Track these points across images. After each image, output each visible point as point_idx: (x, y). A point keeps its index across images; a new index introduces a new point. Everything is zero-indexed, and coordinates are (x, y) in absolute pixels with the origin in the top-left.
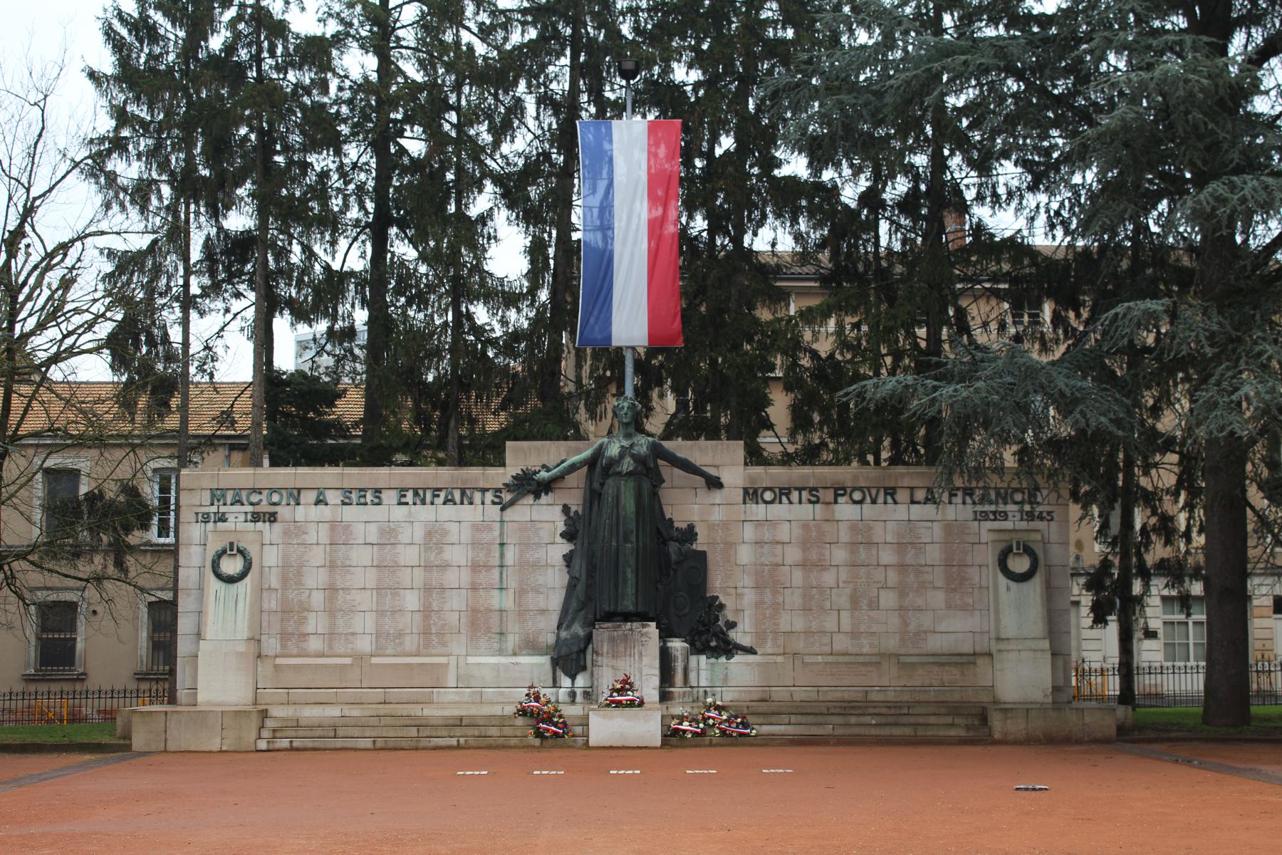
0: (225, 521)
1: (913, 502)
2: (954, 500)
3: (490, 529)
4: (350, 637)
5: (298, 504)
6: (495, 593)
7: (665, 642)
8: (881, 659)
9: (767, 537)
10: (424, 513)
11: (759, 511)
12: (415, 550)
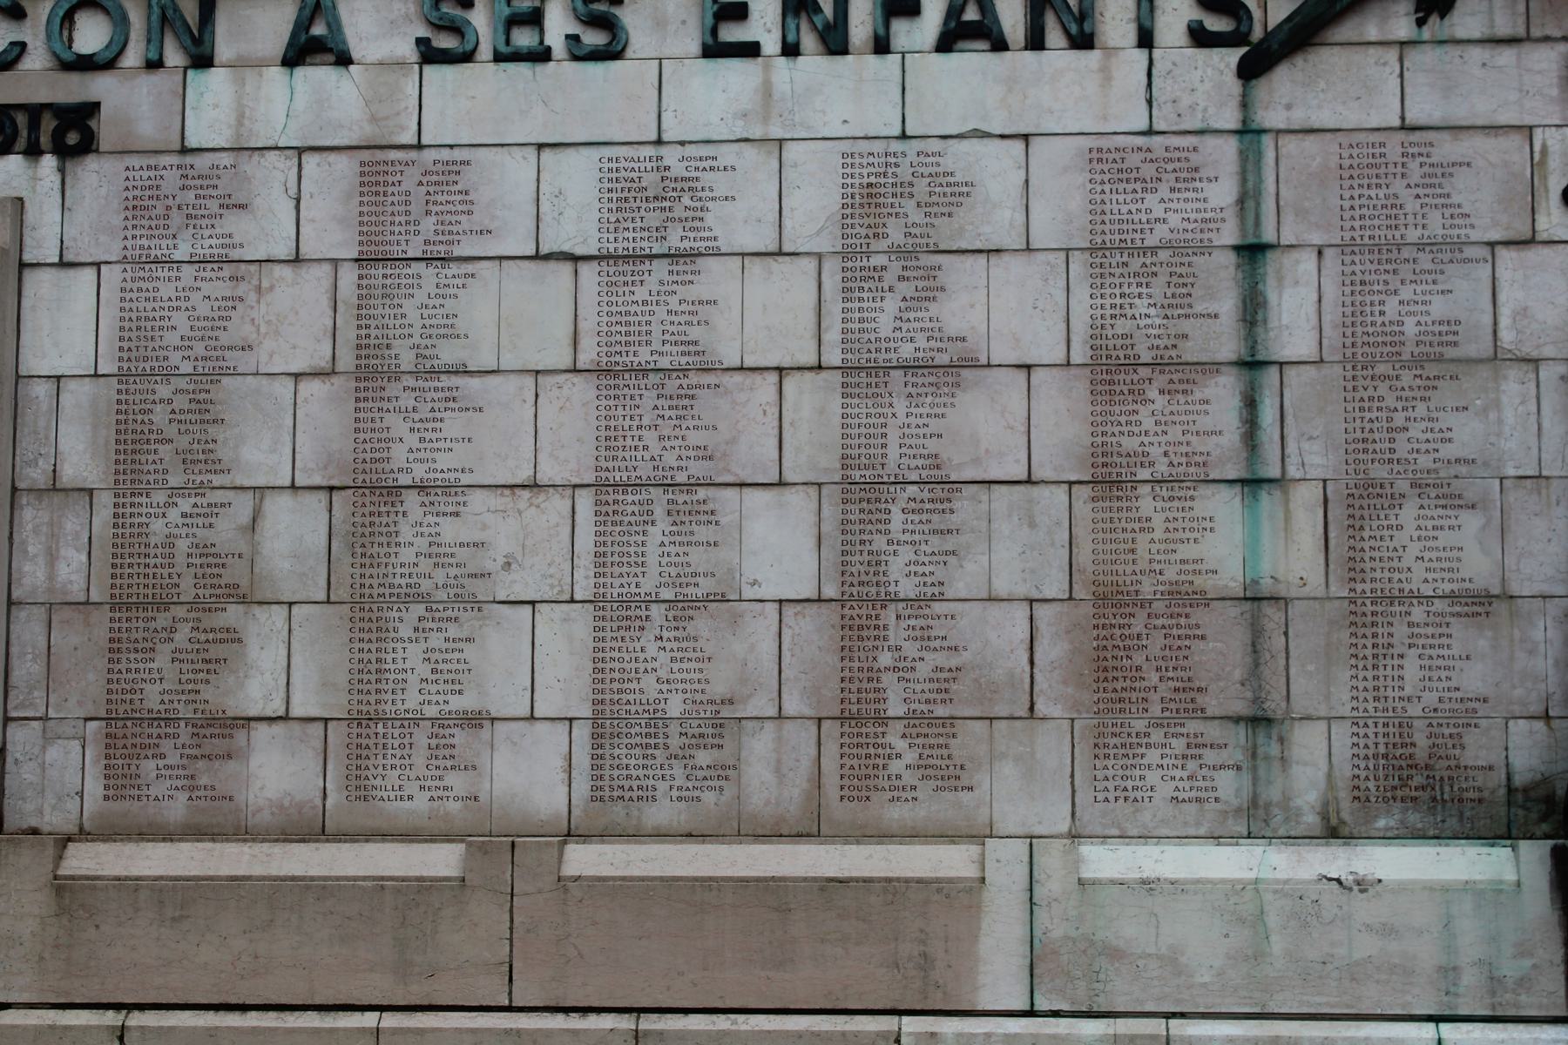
3: (1190, 175)
4: (460, 737)
5: (202, 60)
6: (1223, 506)
12: (795, 281)
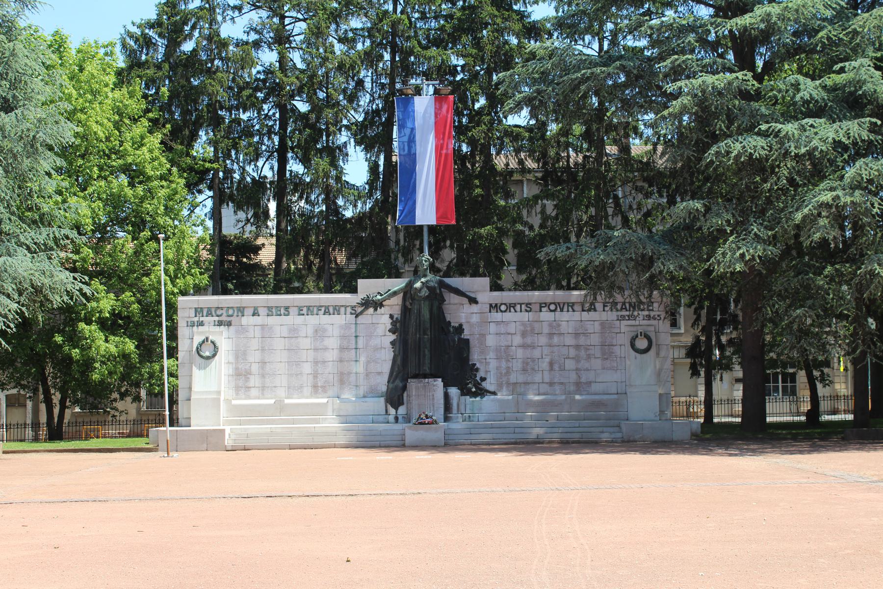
0: (203, 325)
1: (583, 310)
2: (606, 309)
7: (447, 390)
9: (503, 330)
10: (313, 320)
11: (497, 316)
12: (308, 340)
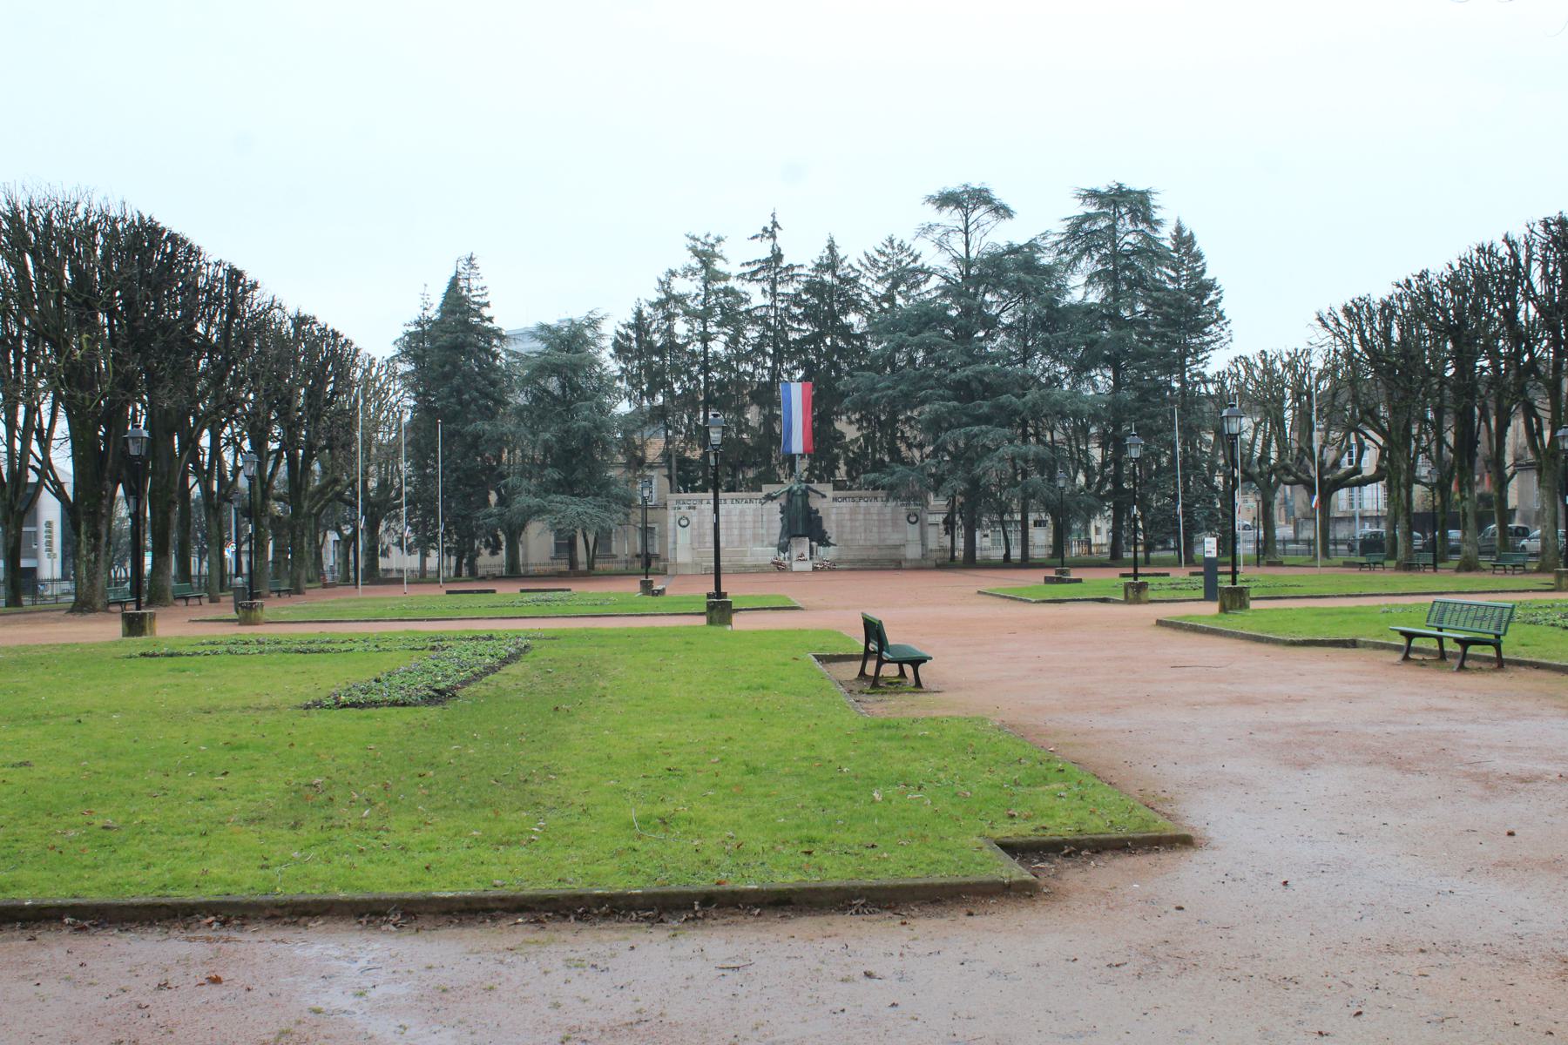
8: (873, 546)
10: (739, 506)
11: (837, 504)
